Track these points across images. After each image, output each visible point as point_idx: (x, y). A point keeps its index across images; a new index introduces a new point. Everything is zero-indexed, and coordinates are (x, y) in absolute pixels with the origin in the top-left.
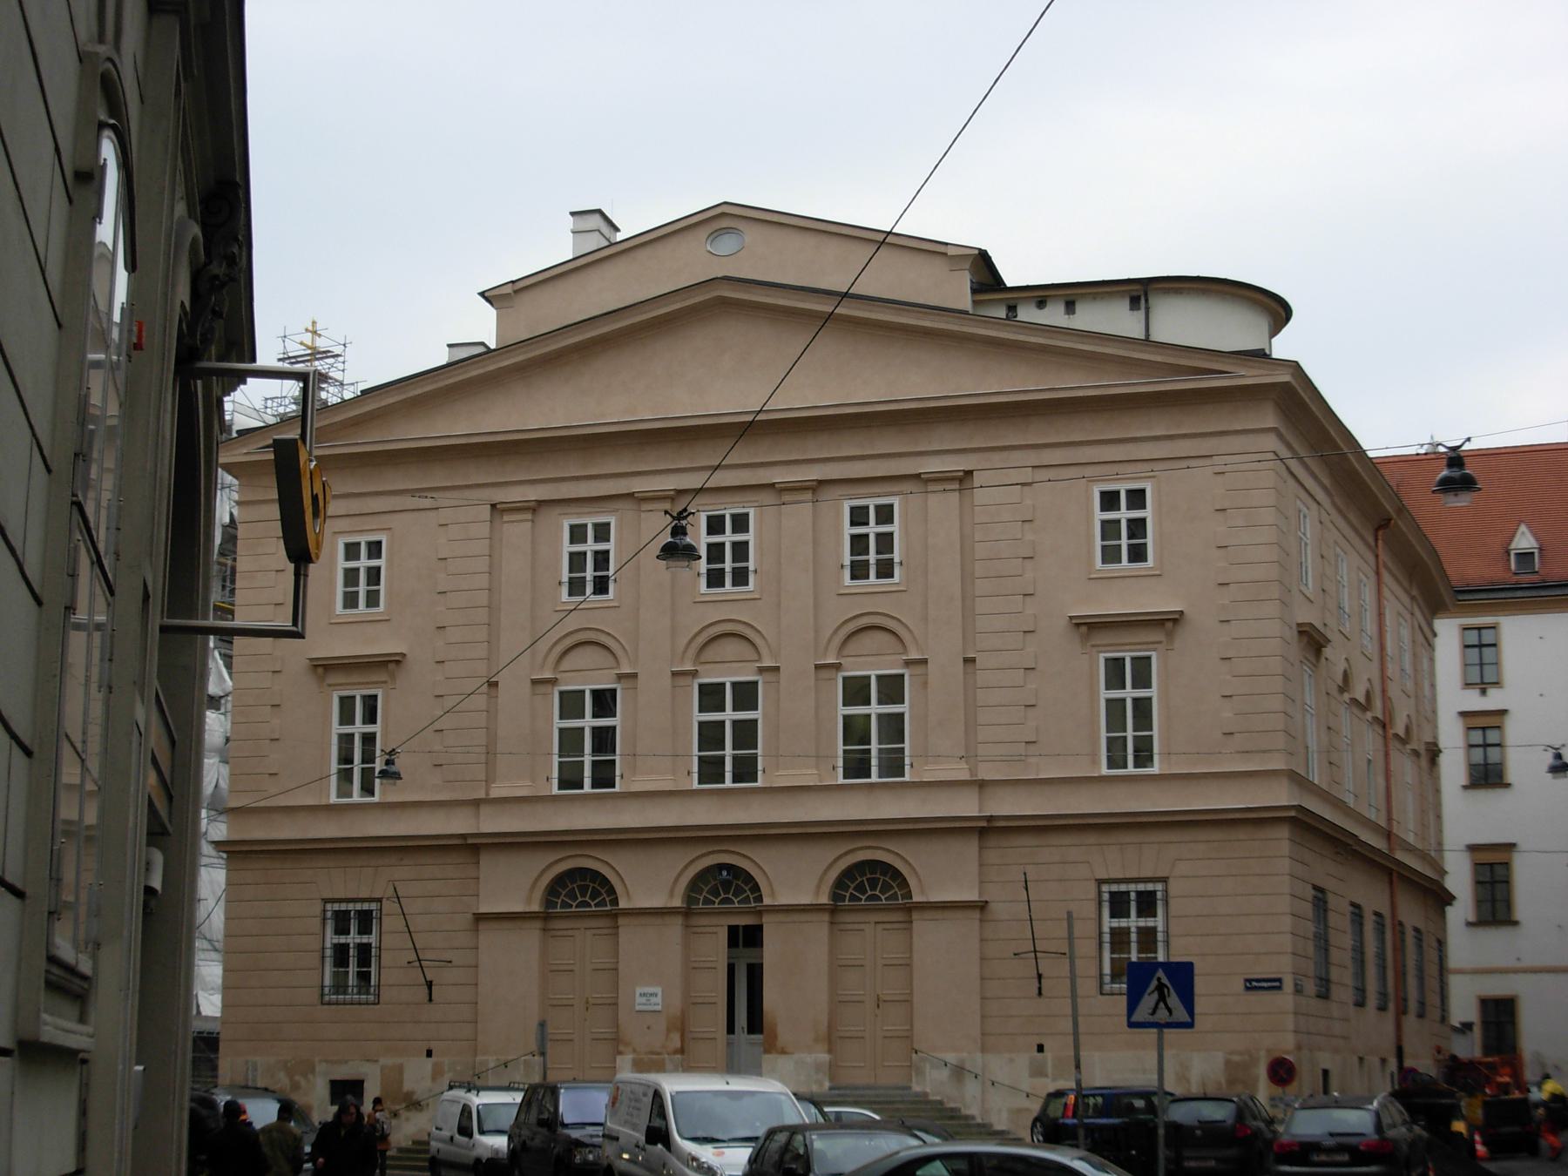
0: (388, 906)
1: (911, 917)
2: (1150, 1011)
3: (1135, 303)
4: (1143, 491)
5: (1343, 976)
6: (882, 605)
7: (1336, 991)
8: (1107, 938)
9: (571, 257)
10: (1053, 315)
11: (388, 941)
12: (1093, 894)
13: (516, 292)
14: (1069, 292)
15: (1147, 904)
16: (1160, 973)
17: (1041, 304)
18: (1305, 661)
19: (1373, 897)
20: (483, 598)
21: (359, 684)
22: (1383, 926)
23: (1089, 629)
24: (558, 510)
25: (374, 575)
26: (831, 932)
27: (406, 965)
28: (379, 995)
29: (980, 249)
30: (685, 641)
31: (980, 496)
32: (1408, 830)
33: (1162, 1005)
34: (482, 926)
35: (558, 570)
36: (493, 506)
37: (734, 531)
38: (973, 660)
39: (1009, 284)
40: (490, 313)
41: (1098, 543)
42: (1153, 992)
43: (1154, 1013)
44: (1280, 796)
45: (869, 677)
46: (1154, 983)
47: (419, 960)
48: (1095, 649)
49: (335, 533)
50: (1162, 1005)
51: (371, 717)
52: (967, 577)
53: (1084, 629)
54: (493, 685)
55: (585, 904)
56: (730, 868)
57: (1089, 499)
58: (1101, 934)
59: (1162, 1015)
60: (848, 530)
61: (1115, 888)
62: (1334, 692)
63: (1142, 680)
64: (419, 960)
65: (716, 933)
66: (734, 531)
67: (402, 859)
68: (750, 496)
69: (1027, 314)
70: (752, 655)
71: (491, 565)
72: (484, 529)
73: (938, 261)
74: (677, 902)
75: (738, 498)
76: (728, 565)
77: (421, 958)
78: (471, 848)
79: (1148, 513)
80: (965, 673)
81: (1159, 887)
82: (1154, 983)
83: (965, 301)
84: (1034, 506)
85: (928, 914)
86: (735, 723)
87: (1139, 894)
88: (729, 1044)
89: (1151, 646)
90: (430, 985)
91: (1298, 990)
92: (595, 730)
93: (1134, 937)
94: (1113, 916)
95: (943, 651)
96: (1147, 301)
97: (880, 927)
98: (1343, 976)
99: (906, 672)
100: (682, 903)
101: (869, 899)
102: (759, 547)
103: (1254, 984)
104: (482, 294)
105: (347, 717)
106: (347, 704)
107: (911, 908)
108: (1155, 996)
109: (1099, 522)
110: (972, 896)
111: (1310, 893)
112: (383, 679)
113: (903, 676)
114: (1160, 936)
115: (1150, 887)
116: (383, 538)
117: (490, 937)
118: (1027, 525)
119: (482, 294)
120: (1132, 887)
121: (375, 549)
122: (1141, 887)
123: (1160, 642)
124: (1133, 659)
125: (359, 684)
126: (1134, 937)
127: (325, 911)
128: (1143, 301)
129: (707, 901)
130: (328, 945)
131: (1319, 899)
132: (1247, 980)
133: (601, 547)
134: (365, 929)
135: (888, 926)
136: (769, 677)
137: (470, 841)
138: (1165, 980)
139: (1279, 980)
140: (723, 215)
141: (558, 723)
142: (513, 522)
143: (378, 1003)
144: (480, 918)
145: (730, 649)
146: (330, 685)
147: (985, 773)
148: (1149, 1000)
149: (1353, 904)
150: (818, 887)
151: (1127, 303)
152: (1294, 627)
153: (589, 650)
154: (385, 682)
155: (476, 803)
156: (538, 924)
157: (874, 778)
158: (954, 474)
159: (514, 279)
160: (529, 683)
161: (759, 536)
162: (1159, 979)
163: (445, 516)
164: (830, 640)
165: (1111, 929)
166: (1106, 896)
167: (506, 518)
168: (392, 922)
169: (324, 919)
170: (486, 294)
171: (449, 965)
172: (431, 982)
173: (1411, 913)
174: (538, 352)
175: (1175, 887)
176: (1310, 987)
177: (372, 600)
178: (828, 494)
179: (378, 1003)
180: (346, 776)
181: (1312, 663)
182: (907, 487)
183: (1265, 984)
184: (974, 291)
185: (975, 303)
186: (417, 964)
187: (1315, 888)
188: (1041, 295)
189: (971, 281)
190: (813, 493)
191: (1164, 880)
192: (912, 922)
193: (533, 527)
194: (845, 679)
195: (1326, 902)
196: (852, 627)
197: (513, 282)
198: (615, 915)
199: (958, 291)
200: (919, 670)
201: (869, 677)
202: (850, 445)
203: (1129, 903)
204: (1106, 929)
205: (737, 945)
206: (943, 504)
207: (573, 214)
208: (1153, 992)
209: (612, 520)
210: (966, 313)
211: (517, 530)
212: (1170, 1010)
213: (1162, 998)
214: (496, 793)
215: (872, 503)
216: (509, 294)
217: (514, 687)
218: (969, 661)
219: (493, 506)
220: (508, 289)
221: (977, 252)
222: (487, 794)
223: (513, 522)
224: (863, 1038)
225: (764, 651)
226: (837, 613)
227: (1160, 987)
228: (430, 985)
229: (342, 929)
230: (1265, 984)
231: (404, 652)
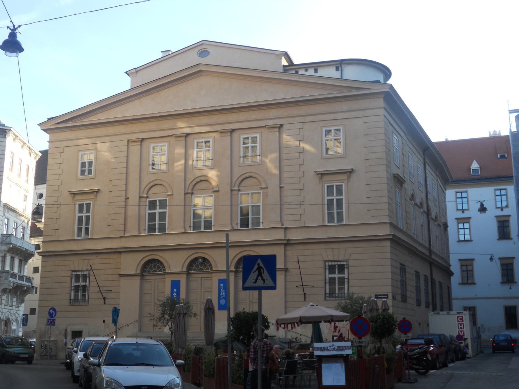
2: (254, 281)
5: (411, 295)
7: (409, 300)
8: (327, 281)
12: (323, 266)
15: (341, 269)
16: (259, 261)
17: (306, 70)
18: (396, 187)
19: (424, 270)
22: (428, 280)
28: (88, 302)
32: (436, 247)
33: (260, 278)
40: (129, 79)
42: (255, 271)
43: (255, 282)
44: (386, 231)
46: (256, 266)
50: (260, 278)
51: (88, 211)
55: (155, 271)
57: (321, 132)
58: (325, 279)
59: (260, 283)
61: (330, 264)
62: (408, 199)
63: (339, 192)
67: (97, 257)
69: (302, 72)
81: (345, 263)
82: (256, 266)
87: (339, 265)
90: (105, 299)
91: (394, 298)
92: (160, 213)
93: (337, 281)
94: (329, 273)
96: (341, 67)
98: (411, 295)
103: (378, 296)
104: (126, 73)
105: (81, 211)
108: (257, 273)
111: (399, 266)
114: (346, 280)
115: (342, 263)
117: (124, 281)
119: (126, 73)
120: (336, 263)
122: (339, 263)
126: (337, 281)
127: (72, 274)
130: (73, 286)
131: (403, 268)
132: (376, 295)
134: (85, 280)
138: (261, 265)
139: (387, 295)
140: (203, 44)
141: (148, 211)
144: (121, 276)
148: (253, 275)
149: (416, 271)
151: (334, 68)
152: (392, 175)
153: (158, 186)
162: (259, 264)
165: (329, 278)
166: (327, 267)
168: (92, 278)
171: (111, 292)
172: (105, 297)
173: (438, 276)
175: (351, 263)
176: (399, 298)
180: (80, 230)
181: (400, 189)
183: (382, 297)
187: (401, 264)
188: (306, 66)
191: (347, 261)
195: (405, 269)
200: (265, 190)
204: (327, 278)
207: (162, 52)
208: (255, 271)
212: (264, 281)
213: (260, 274)
214: (127, 234)
227: (259, 268)
228: (105, 299)
229: (77, 281)
230: (382, 297)
231: (99, 189)
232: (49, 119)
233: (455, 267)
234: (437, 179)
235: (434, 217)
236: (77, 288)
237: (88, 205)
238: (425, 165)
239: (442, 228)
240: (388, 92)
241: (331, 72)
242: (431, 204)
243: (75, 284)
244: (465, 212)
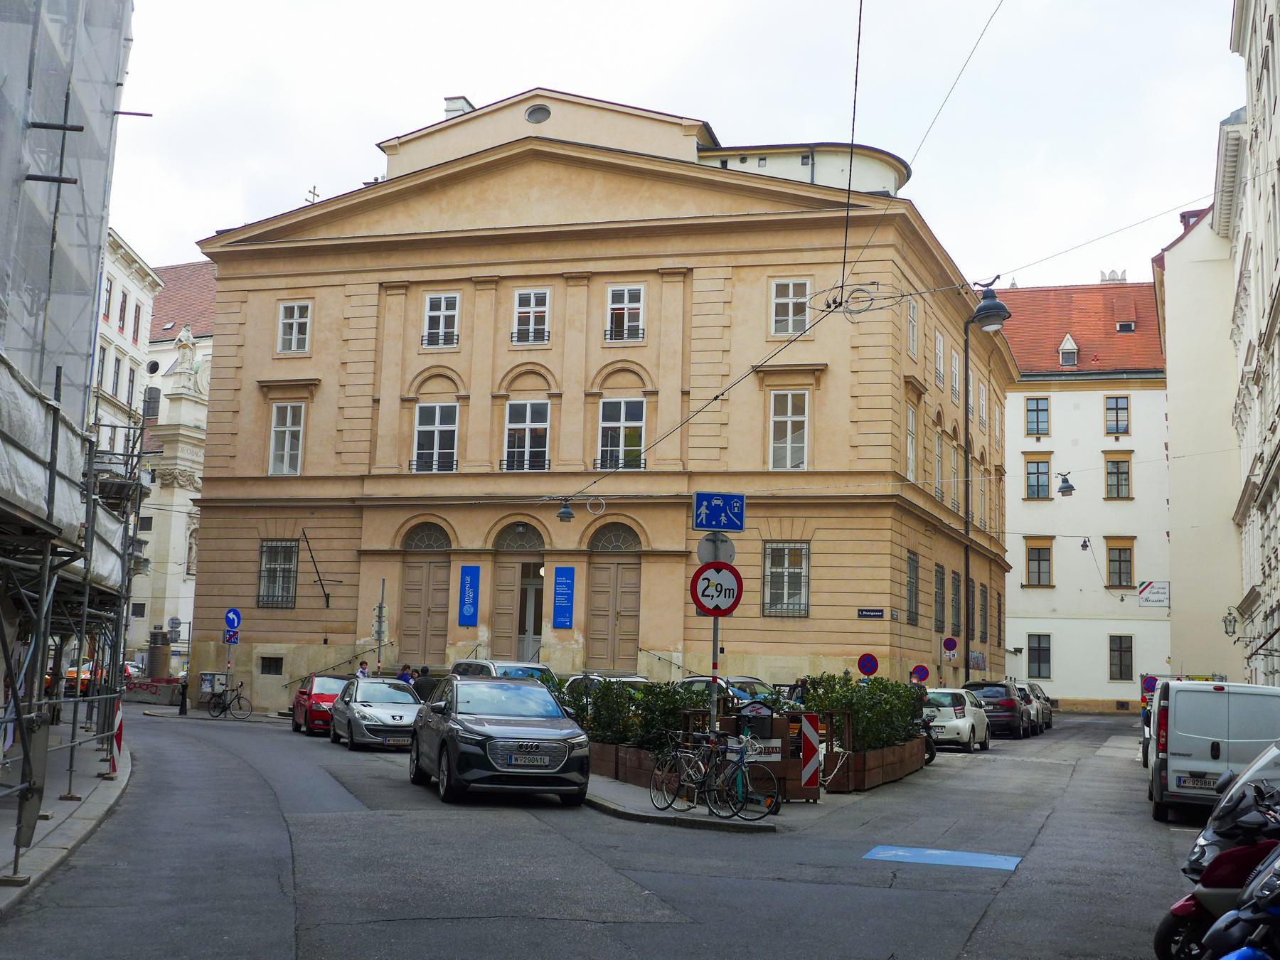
0: (303, 545)
1: (640, 561)
3: (805, 159)
4: (805, 285)
5: (927, 611)
6: (444, 361)
7: (922, 621)
8: (768, 579)
9: (445, 119)
10: (752, 166)
11: (301, 567)
12: (760, 550)
13: (400, 144)
14: (742, 152)
15: (796, 557)
17: (743, 160)
18: (908, 401)
19: (952, 560)
20: (371, 345)
21: (290, 398)
22: (959, 581)
23: (764, 374)
24: (423, 288)
25: (302, 328)
26: (589, 569)
27: (313, 583)
28: (295, 602)
29: (703, 122)
30: (411, 379)
31: (697, 285)
34: (362, 558)
35: (421, 327)
36: (381, 284)
37: (537, 305)
38: (688, 393)
39: (723, 145)
40: (383, 157)
41: (773, 318)
44: (885, 487)
45: (435, 407)
47: (320, 580)
48: (768, 388)
49: (279, 300)
51: (296, 421)
52: (686, 338)
53: (761, 375)
54: (376, 401)
56: (525, 525)
57: (768, 289)
60: (428, 313)
61: (774, 546)
62: (930, 423)
63: (799, 409)
64: (320, 580)
65: (422, 567)
66: (537, 305)
67: (313, 514)
68: (548, 282)
69: (734, 165)
70: (453, 388)
71: (378, 323)
72: (374, 300)
73: (676, 129)
74: (489, 546)
75: (540, 282)
76: (442, 330)
77: (321, 578)
78: (357, 507)
79: (456, 313)
80: (682, 401)
81: (804, 546)
83: (692, 156)
84: (732, 293)
85: (651, 559)
86: (441, 432)
87: (790, 550)
88: (520, 641)
89: (805, 387)
90: (327, 597)
91: (894, 619)
93: (786, 579)
94: (773, 564)
95: (669, 388)
96: (813, 159)
97: (432, 564)
98: (927, 611)
99: (645, 400)
100: (401, 547)
101: (427, 546)
102: (553, 317)
103: (864, 613)
104: (378, 145)
105: (282, 420)
106: (282, 412)
107: (641, 555)
109: (428, 317)
110: (682, 548)
111: (905, 554)
112: (307, 396)
113: (547, 404)
114: (803, 579)
115: (798, 546)
116: (309, 303)
117: (366, 566)
118: (726, 305)
119: (378, 145)
120: (786, 546)
121: (303, 310)
122: (792, 546)
123: (812, 385)
124: (793, 395)
125: (290, 398)
126: (786, 579)
127: (262, 546)
128: (810, 157)
129: (417, 546)
130: (263, 568)
131: (913, 560)
132: (859, 610)
133: (450, 313)
135: (625, 566)
136: (556, 401)
137: (357, 503)
139: (881, 611)
140: (538, 96)
142: (393, 295)
143: (294, 608)
144: (362, 553)
145: (434, 386)
146: (271, 399)
147: (692, 467)
149: (937, 565)
150: (581, 539)
151: (800, 160)
152: (902, 378)
153: (440, 380)
154: (307, 398)
155: (362, 478)
156: (399, 558)
157: (435, 471)
158: (681, 270)
159: (399, 136)
160: (398, 401)
161: (552, 308)
163: (349, 290)
164: (595, 378)
165: (772, 573)
166: (768, 551)
167: (389, 292)
168: (304, 555)
169: (262, 552)
170: (381, 145)
171: (341, 584)
172: (329, 594)
173: (980, 573)
174: (415, 183)
175: (814, 547)
176: (903, 617)
177: (301, 343)
178: (414, 291)
179: (294, 608)
180: (280, 459)
181: (915, 404)
182: (651, 278)
183: (872, 614)
184: (699, 150)
185: (700, 157)
186: (319, 583)
187: (909, 551)
188: (743, 153)
189: (698, 143)
190: (588, 281)
191: (808, 542)
192: (450, 562)
193: (406, 300)
194: (511, 406)
195: (917, 562)
196: (610, 369)
197: (398, 138)
198: (449, 554)
199: (686, 149)
200: (653, 399)
201: (435, 407)
202: (538, 252)
203: (784, 556)
204: (768, 573)
205: (529, 577)
206: (673, 291)
209: (458, 295)
210: (694, 164)
211: (395, 301)
214: (375, 472)
215: (443, 296)
216: (396, 145)
217: (390, 404)
218: (685, 393)
219: (381, 284)
220: (395, 142)
221: (701, 123)
222: (370, 472)
223: (393, 295)
224: (606, 639)
225: (461, 387)
226: (601, 358)
228: (327, 597)
230: (872, 614)
231: (319, 378)
232: (220, 233)
233: (1016, 554)
234: (990, 378)
235: (977, 456)
236: (272, 574)
237: (296, 411)
238: (966, 352)
239: (993, 477)
240: (903, 215)
241: (792, 169)
242: (974, 429)
243: (268, 566)
244: (1043, 439)
